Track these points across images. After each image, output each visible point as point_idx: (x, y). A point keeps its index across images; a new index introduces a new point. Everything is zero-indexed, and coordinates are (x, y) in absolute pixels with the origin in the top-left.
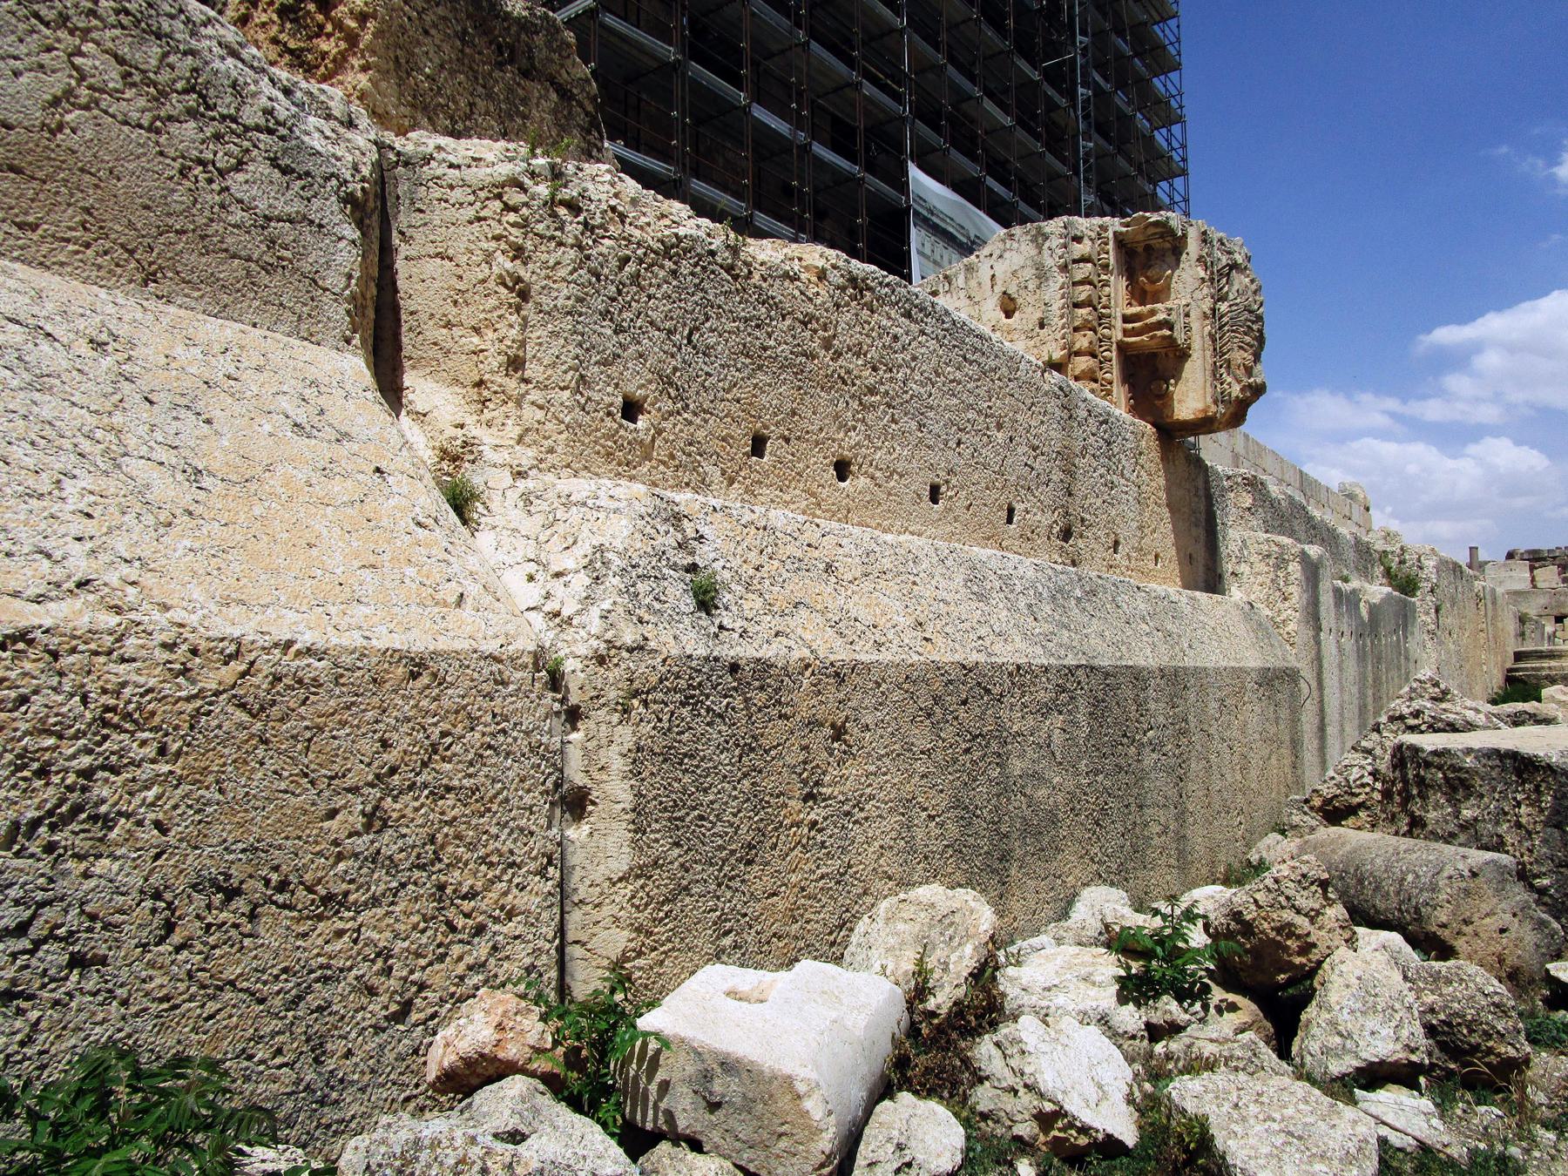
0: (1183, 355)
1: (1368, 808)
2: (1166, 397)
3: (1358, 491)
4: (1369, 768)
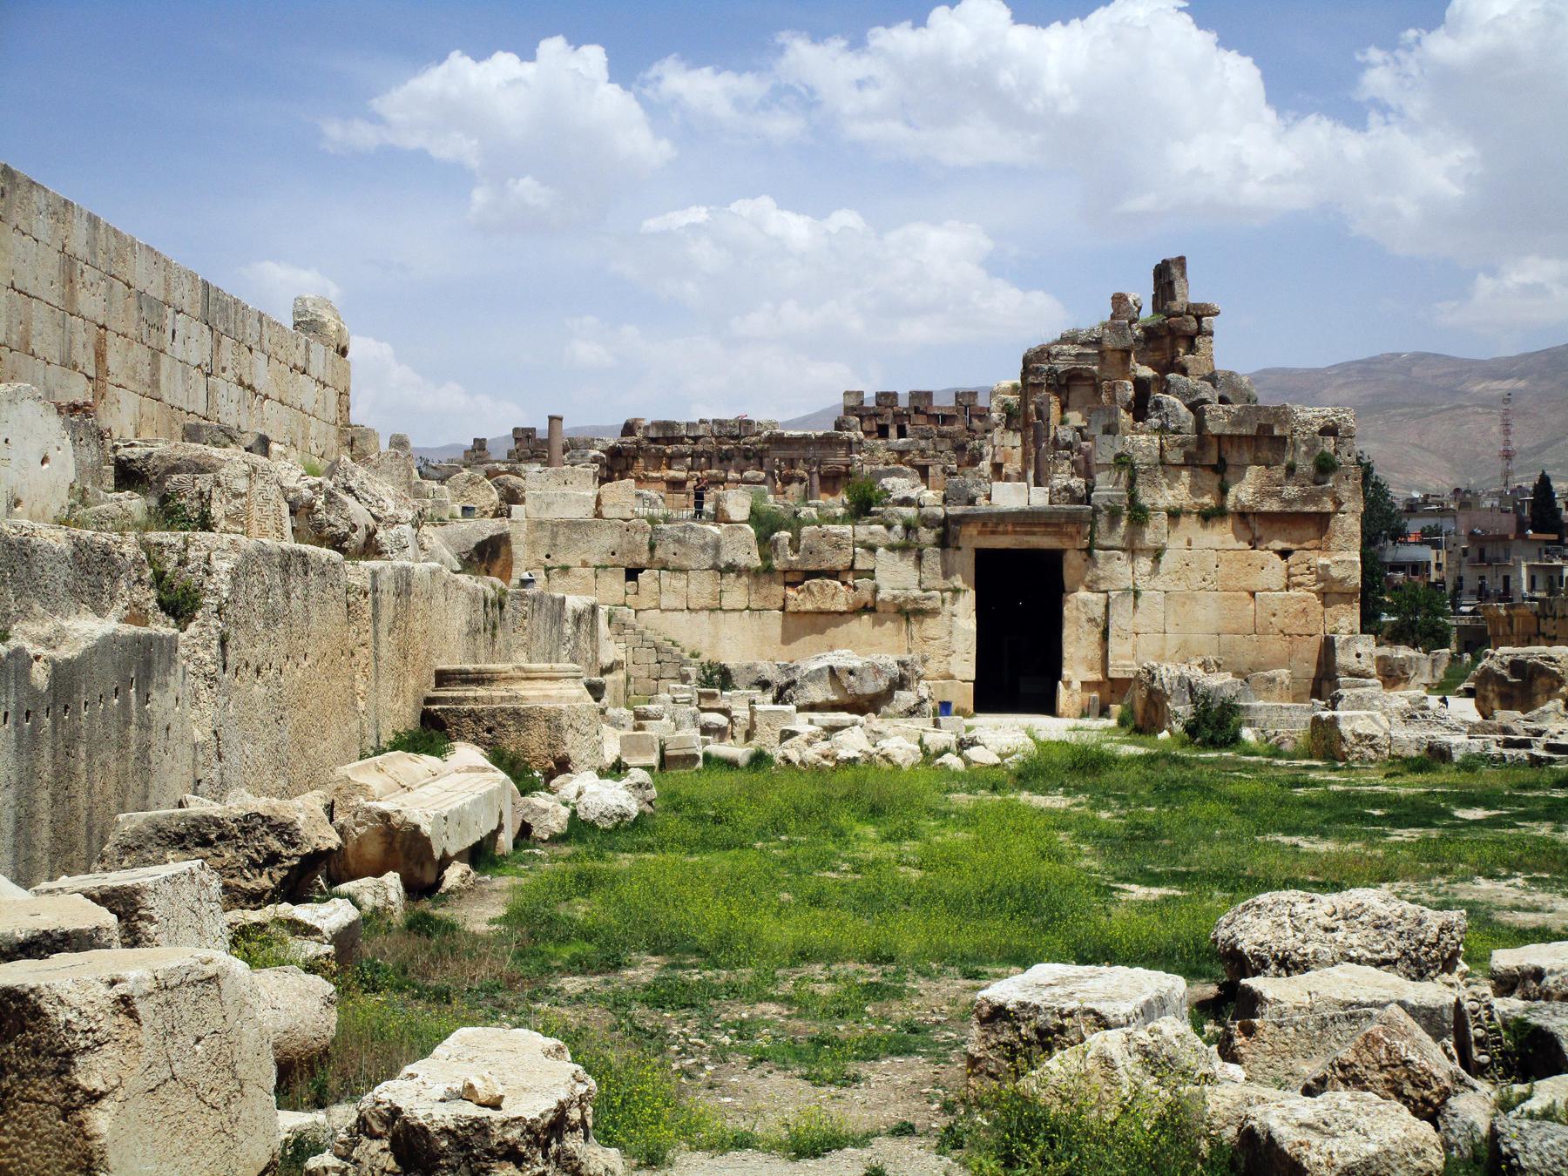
3: (327, 316)
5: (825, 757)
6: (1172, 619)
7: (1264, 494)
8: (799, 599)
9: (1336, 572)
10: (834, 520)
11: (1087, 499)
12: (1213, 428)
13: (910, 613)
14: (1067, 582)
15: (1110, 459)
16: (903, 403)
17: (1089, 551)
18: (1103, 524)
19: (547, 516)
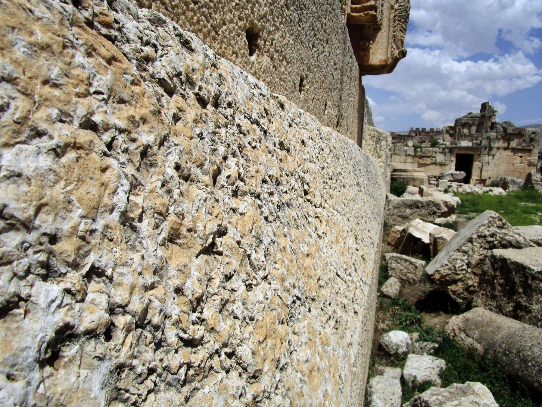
0: (377, 28)
1: (463, 281)
2: (366, 50)
4: (466, 261)
7: (518, 145)
8: (421, 161)
9: (532, 161)
12: (509, 132)
13: (442, 165)
16: (420, 130)
17: (479, 155)
18: (483, 150)
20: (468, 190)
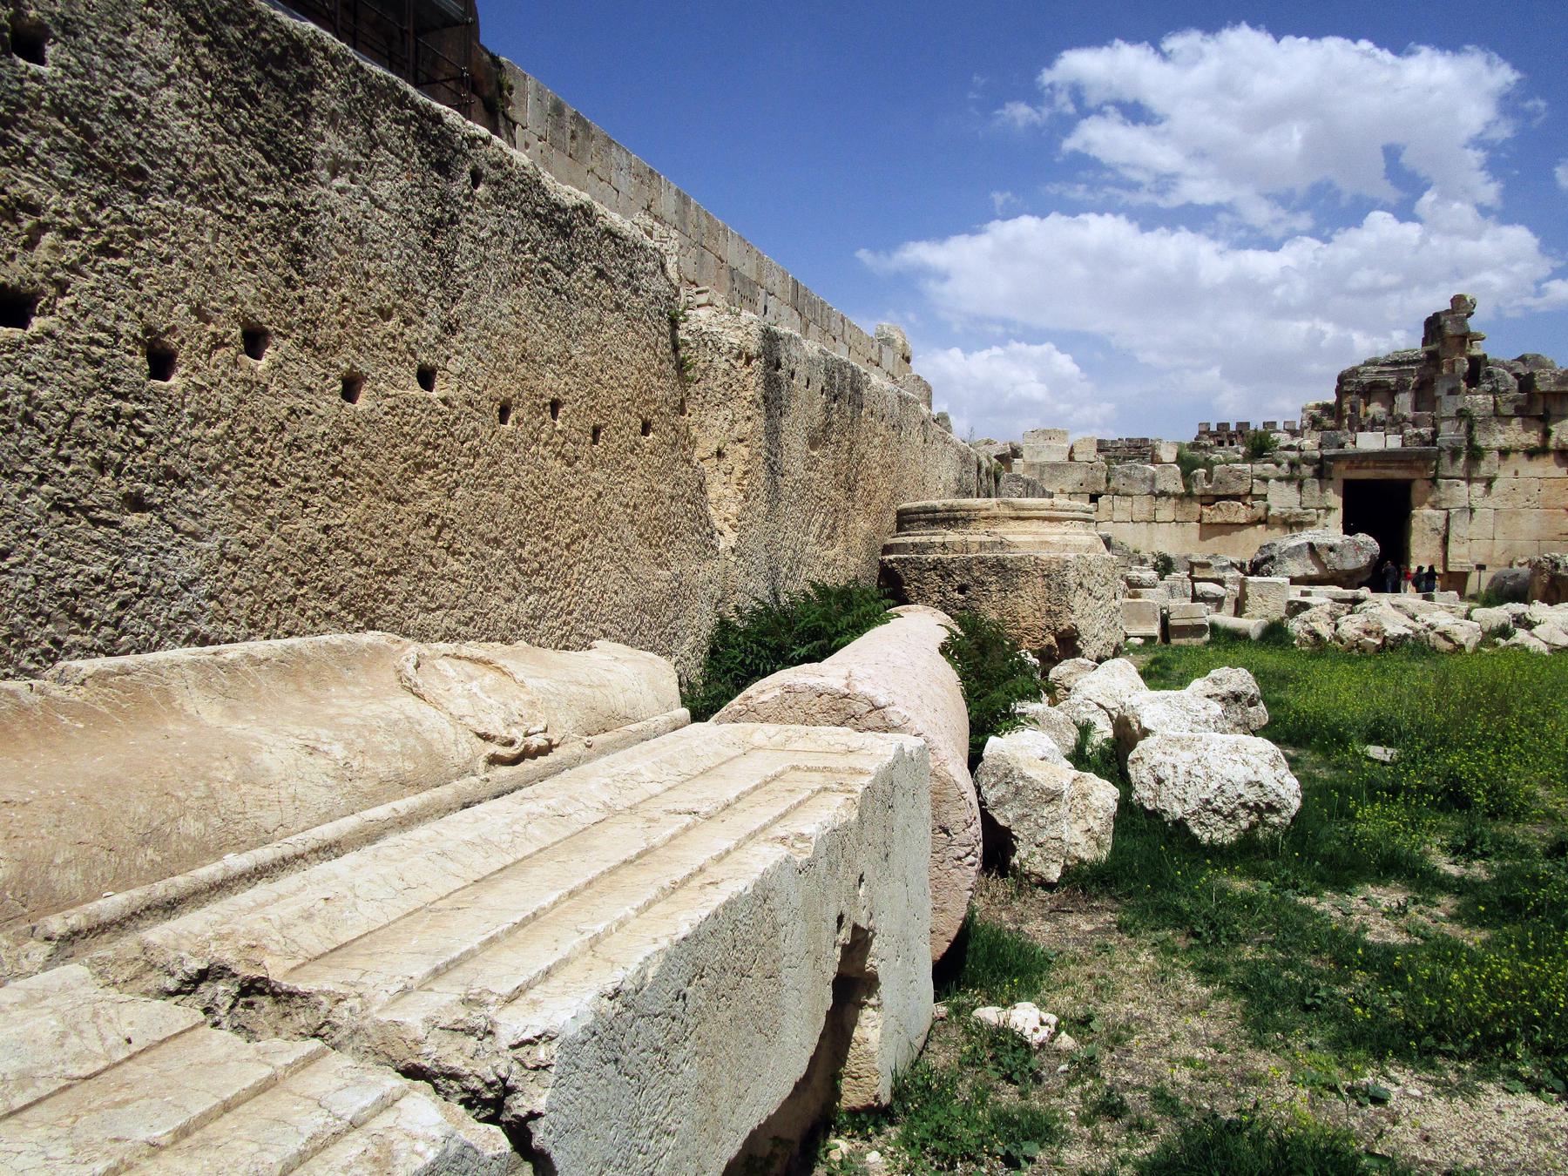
5: (1368, 633)
6: (1500, 529)
8: (1213, 515)
10: (1237, 461)
11: (1434, 443)
12: (1541, 387)
14: (1414, 502)
15: (1453, 413)
16: (1233, 428)
17: (1433, 481)
18: (1446, 460)
19: (1036, 460)
20: (1396, 626)
